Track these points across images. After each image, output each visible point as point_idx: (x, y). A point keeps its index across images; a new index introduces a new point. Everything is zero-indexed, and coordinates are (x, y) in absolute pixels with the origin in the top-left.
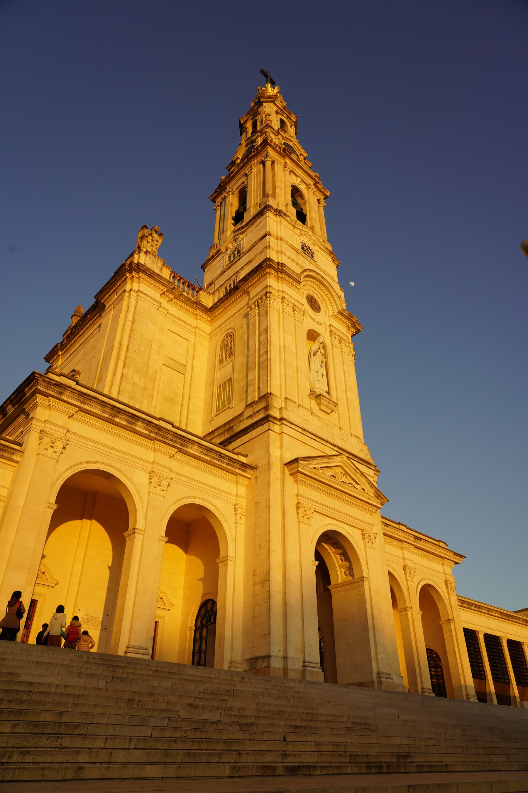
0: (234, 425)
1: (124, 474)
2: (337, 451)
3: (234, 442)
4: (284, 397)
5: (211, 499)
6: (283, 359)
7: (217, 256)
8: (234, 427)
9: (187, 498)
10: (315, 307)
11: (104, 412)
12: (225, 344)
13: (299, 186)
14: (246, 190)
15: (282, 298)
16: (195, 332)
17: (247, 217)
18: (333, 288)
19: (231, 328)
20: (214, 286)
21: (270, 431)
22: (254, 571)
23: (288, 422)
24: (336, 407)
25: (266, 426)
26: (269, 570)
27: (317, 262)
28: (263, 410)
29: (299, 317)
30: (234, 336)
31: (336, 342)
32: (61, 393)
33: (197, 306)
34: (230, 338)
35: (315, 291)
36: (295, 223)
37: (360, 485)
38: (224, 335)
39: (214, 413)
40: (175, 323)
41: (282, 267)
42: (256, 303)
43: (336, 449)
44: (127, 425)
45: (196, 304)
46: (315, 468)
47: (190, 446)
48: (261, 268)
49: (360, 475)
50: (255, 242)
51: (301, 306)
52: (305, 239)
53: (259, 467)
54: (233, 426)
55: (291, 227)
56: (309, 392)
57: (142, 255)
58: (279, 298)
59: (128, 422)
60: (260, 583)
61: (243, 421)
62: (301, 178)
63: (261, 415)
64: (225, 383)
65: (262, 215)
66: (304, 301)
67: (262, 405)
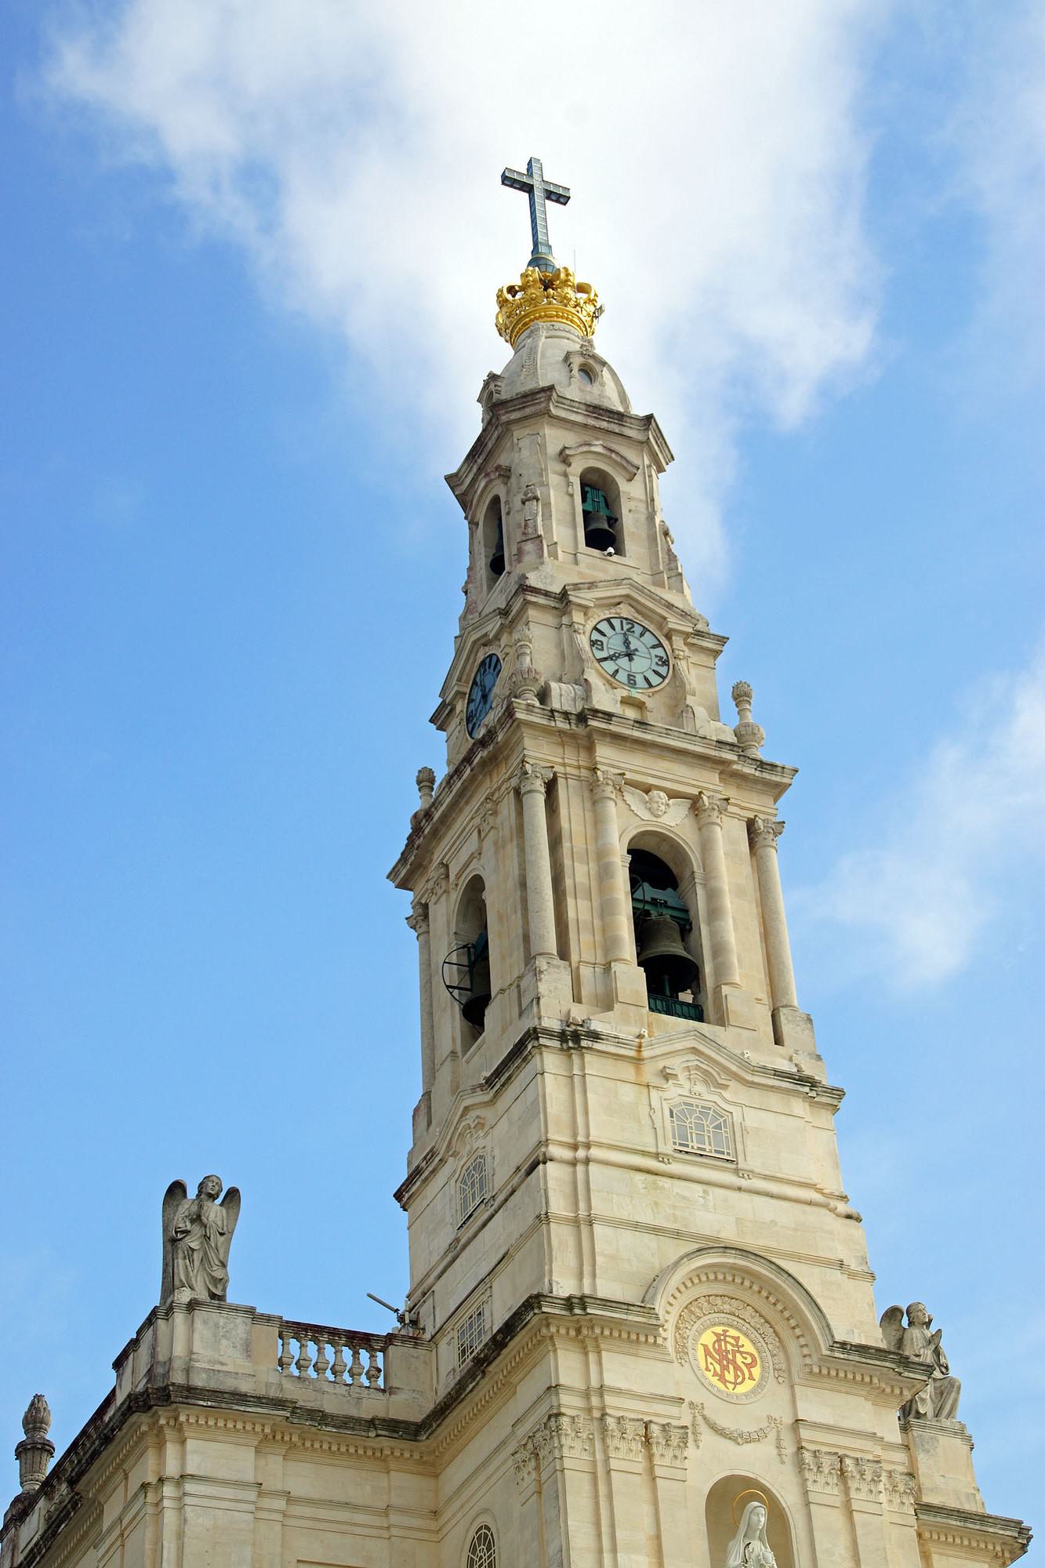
10: (737, 1368)
14: (483, 897)
16: (388, 1528)
18: (790, 1275)
19: (485, 1511)
29: (667, 1461)
31: (825, 1489)
33: (380, 1432)
36: (640, 1047)
38: (472, 1533)
40: (318, 1525)
45: (376, 1429)
48: (525, 1326)
50: (518, 1169)
55: (628, 1071)
57: (179, 1317)
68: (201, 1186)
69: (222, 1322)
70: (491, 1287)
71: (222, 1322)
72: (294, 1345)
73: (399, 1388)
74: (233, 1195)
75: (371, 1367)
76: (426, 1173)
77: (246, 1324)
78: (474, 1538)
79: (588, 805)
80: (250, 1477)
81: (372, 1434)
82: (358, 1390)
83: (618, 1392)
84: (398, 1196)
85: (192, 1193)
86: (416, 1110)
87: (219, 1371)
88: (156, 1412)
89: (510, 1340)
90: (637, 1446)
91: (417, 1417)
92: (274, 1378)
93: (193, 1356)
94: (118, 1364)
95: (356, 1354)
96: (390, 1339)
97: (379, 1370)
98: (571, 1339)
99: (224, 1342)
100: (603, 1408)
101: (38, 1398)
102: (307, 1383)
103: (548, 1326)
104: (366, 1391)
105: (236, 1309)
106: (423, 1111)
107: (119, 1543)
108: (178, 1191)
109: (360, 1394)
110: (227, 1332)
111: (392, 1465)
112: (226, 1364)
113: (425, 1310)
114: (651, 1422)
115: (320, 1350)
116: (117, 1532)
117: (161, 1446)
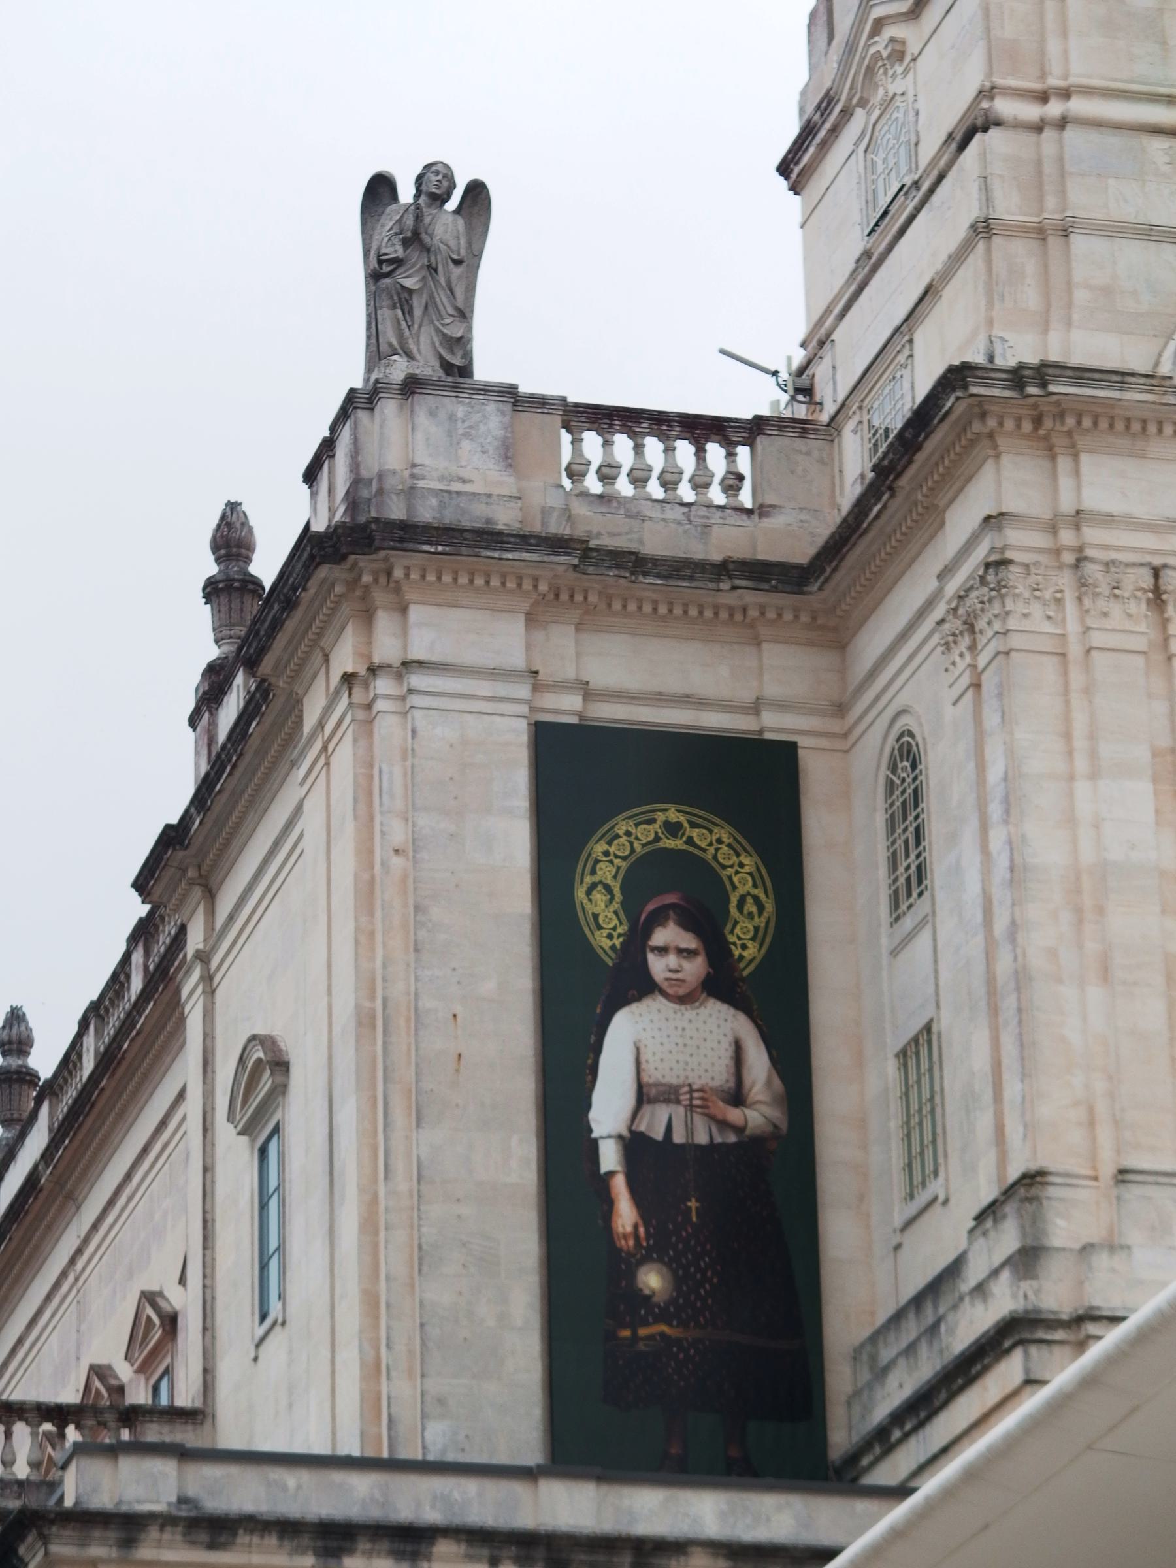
15: (1079, 560)
32: (128, 1543)
33: (738, 582)
45: (730, 577)
58: (1061, 567)
64: (916, 1040)
68: (419, 180)
70: (911, 341)
71: (460, 411)
72: (592, 441)
73: (774, 506)
74: (477, 193)
75: (728, 472)
76: (822, 134)
77: (503, 413)
80: (518, 660)
81: (725, 586)
82: (703, 511)
83: (1108, 520)
84: (784, 169)
85: (406, 193)
86: (813, 15)
87: (458, 493)
88: (355, 564)
89: (926, 438)
90: (1139, 608)
91: (802, 552)
92: (554, 501)
93: (416, 471)
94: (311, 476)
95: (700, 453)
96: (756, 428)
97: (741, 478)
98: (1027, 437)
99: (466, 445)
100: (1080, 549)
101: (233, 506)
102: (615, 504)
103: (983, 416)
104: (719, 514)
105: (487, 390)
106: (822, 19)
108: (384, 190)
109: (708, 518)
110: (471, 427)
111: (764, 631)
112: (470, 481)
113: (821, 371)
114: (1165, 566)
115: (638, 449)
116: (318, 745)
117: (367, 617)
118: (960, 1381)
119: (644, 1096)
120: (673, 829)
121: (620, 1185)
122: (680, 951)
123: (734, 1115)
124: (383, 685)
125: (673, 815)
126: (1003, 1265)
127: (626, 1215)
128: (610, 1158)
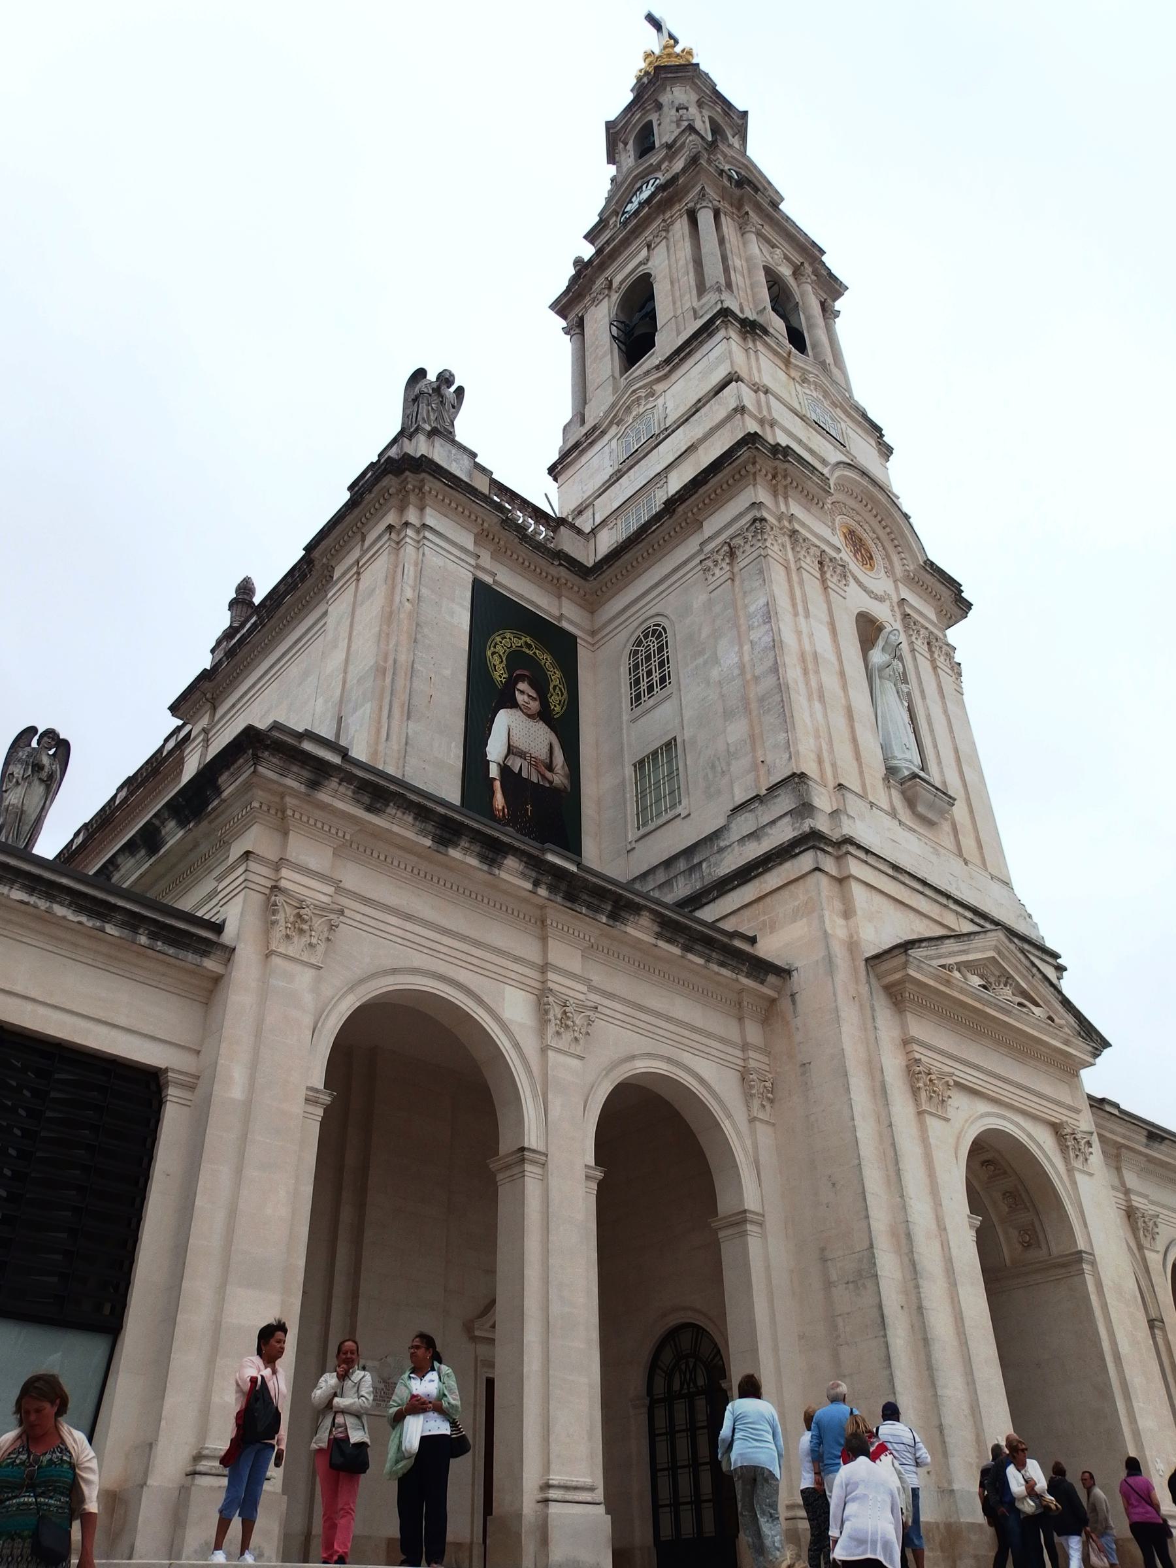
0: (704, 860)
1: (480, 1001)
2: (972, 921)
3: (711, 905)
4: (831, 784)
5: (687, 1058)
6: (814, 684)
7: (589, 441)
8: (704, 865)
9: (633, 1058)
11: (423, 833)
12: (642, 656)
13: (779, 268)
17: (666, 342)
20: (594, 514)
21: (817, 873)
22: (823, 1250)
23: (859, 847)
24: (953, 805)
25: (806, 861)
26: (871, 1246)
27: (848, 447)
28: (787, 819)
29: (835, 579)
30: (666, 633)
32: (314, 785)
34: (657, 639)
35: (858, 518)
37: (1041, 1007)
38: (639, 632)
39: (632, 835)
41: (785, 457)
42: (726, 548)
43: (969, 915)
44: (477, 866)
45: (559, 559)
46: (943, 966)
47: (631, 918)
49: (1040, 979)
50: (699, 401)
51: (833, 554)
52: (814, 391)
53: (797, 969)
54: (700, 863)
56: (883, 771)
59: (483, 858)
60: (848, 1283)
61: (729, 850)
62: (783, 251)
63: (784, 833)
64: (655, 753)
65: (711, 335)
66: (838, 540)
67: (785, 802)
69: (453, 451)
70: (666, 477)
71: (453, 451)
74: (460, 391)
78: (650, 627)
79: (739, 234)
81: (556, 563)
89: (712, 477)
98: (767, 481)
99: (454, 463)
107: (355, 577)
111: (564, 592)
116: (355, 569)
118: (761, 870)
119: (511, 750)
120: (529, 646)
121: (497, 784)
122: (529, 696)
123: (548, 775)
124: (410, 532)
125: (529, 641)
126: (785, 814)
127: (499, 801)
128: (494, 772)
